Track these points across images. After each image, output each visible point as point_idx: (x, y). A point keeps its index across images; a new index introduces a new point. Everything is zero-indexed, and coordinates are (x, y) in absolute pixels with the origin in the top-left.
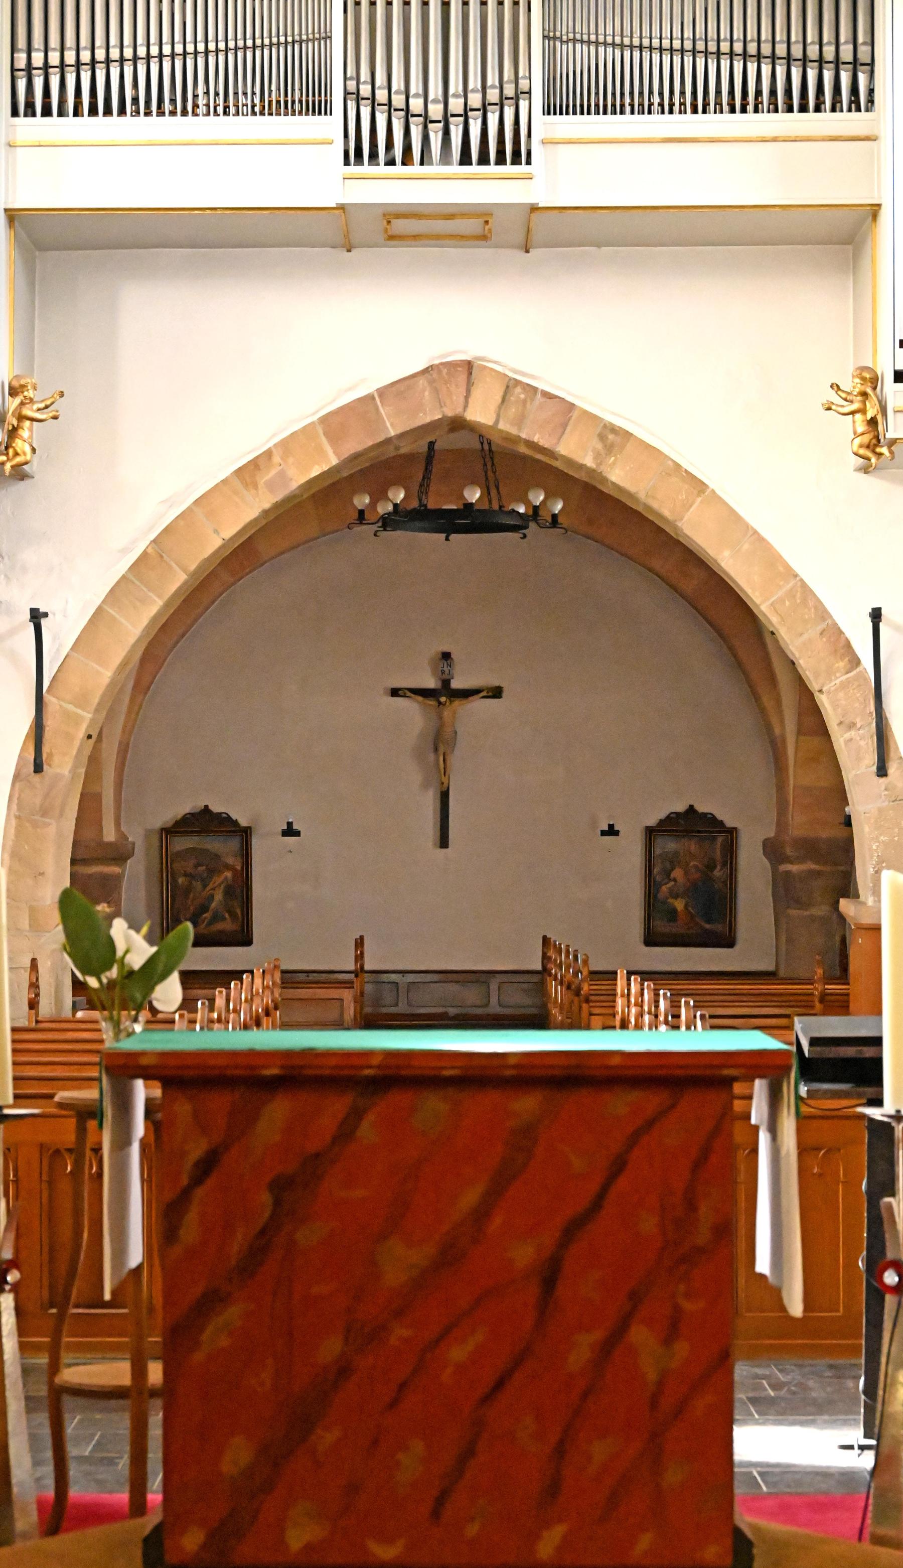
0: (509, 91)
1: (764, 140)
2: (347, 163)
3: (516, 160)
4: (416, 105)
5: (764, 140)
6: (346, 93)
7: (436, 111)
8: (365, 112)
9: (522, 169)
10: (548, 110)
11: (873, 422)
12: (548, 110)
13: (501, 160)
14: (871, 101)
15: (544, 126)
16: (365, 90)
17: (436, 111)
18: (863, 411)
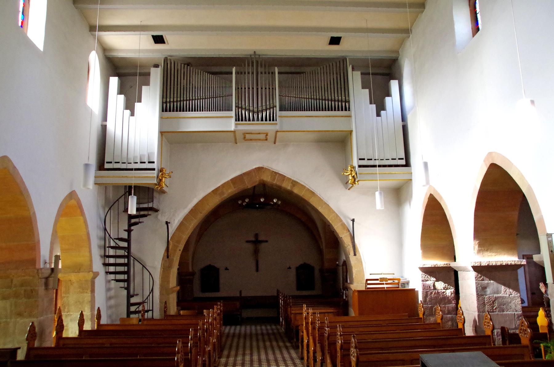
0: (272, 106)
1: (327, 117)
2: (236, 121)
3: (273, 120)
4: (251, 108)
5: (327, 117)
6: (236, 107)
7: (255, 110)
8: (240, 110)
9: (275, 122)
10: (281, 110)
11: (353, 177)
12: (281, 110)
13: (270, 120)
14: (349, 110)
15: (279, 113)
16: (240, 106)
17: (255, 110)
18: (351, 174)
